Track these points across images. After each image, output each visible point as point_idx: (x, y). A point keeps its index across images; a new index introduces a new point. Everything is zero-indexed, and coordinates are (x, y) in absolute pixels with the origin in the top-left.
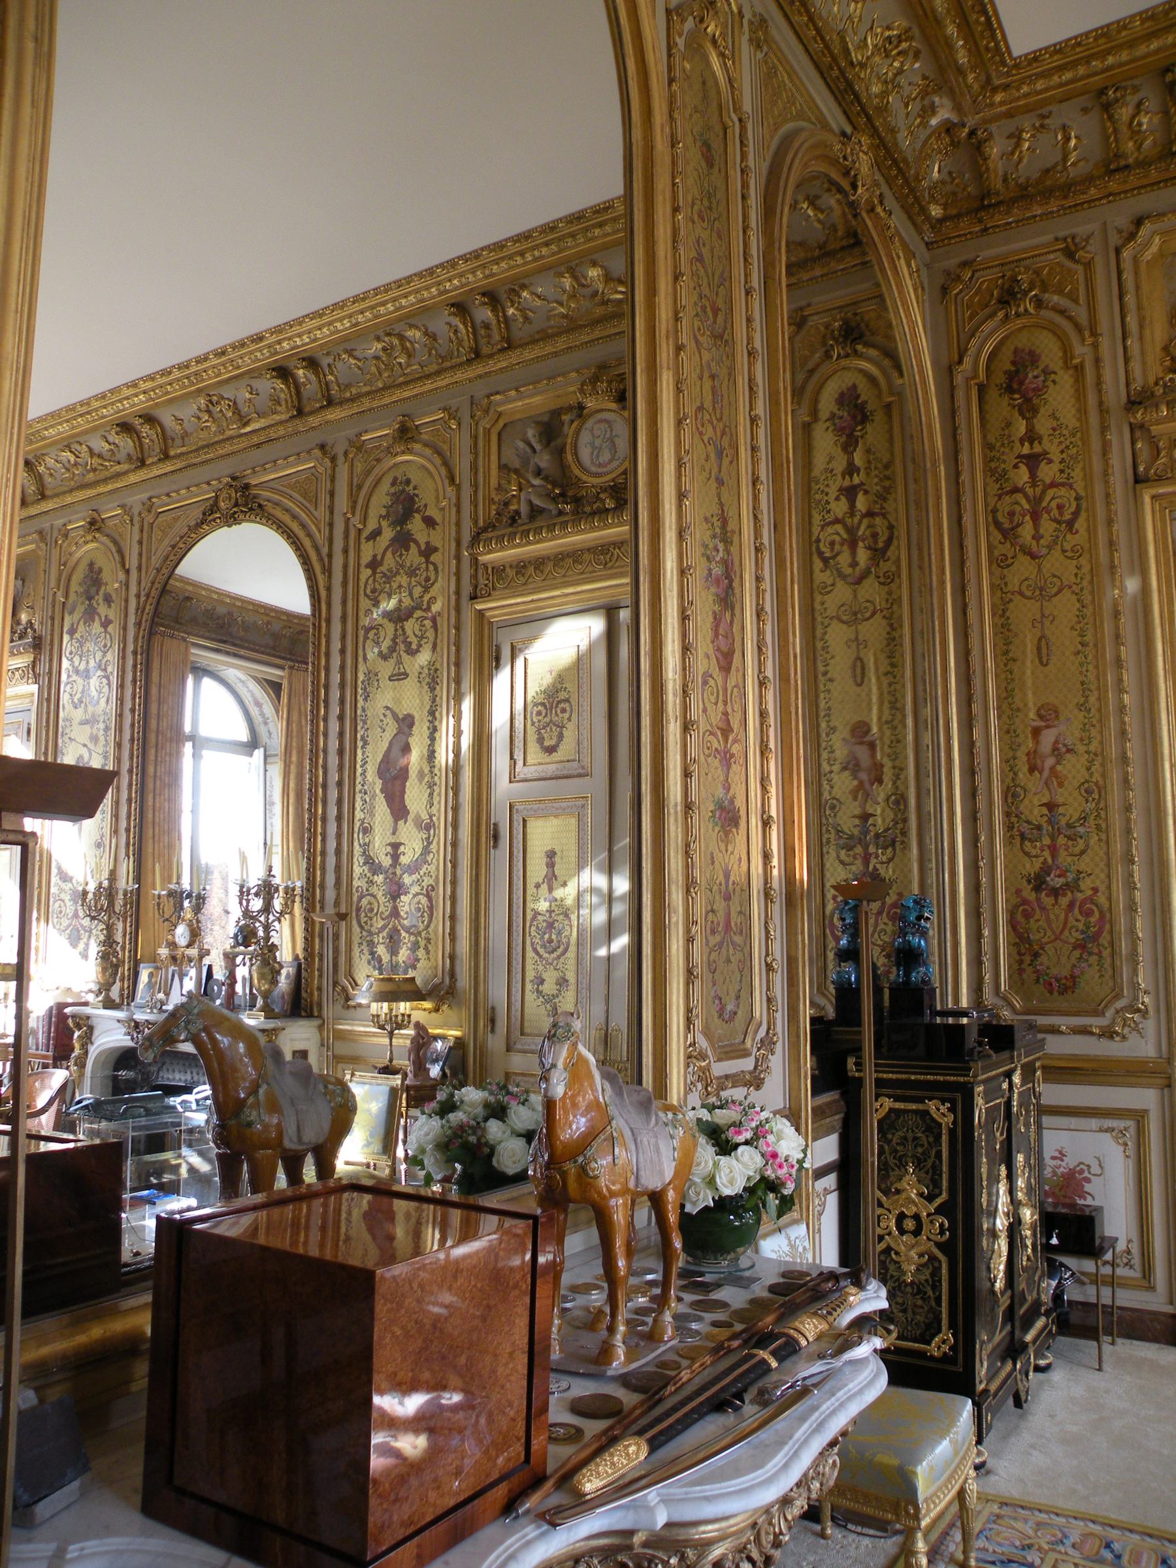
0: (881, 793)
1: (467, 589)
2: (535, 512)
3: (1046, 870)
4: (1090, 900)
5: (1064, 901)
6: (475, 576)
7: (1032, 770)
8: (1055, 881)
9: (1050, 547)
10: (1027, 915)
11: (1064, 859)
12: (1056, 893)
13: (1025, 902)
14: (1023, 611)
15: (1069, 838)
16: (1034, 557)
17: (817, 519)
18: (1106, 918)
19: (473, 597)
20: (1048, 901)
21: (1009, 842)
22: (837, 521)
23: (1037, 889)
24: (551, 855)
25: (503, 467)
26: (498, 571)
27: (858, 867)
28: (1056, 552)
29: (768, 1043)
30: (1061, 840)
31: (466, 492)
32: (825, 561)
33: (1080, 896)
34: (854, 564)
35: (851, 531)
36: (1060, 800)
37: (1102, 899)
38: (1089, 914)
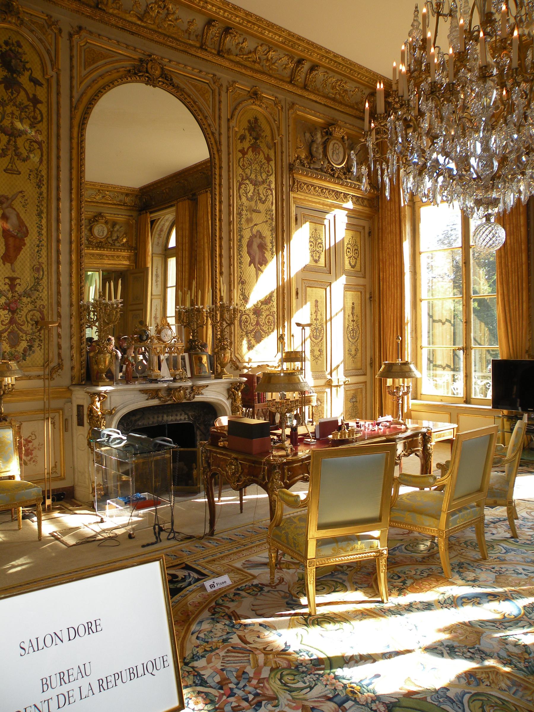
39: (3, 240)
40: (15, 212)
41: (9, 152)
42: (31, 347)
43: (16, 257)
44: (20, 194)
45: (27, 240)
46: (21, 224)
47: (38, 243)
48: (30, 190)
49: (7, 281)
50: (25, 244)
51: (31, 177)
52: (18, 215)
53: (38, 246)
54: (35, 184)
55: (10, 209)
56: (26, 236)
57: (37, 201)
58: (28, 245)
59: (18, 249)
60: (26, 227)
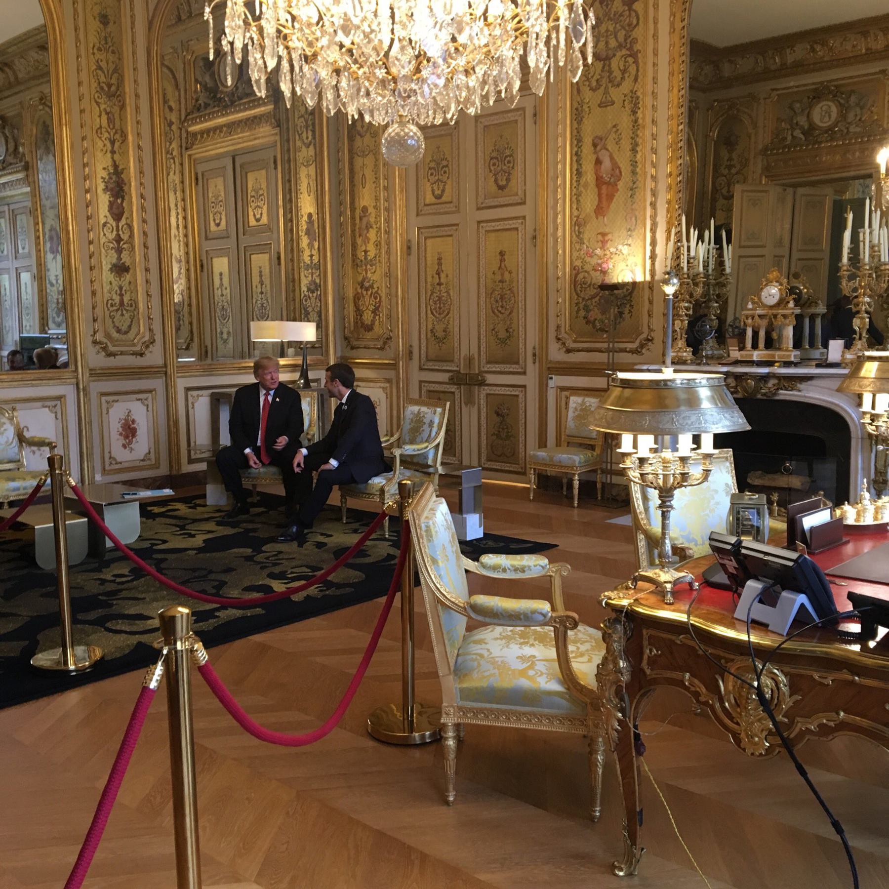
0: (316, 245)
1: (184, 145)
2: (207, 105)
3: (364, 280)
4: (377, 292)
5: (369, 293)
6: (187, 138)
7: (360, 236)
8: (367, 284)
9: (366, 132)
10: (359, 299)
11: (369, 275)
12: (367, 289)
13: (358, 293)
14: (358, 162)
15: (371, 266)
16: (361, 136)
17: (296, 116)
18: (380, 301)
19: (187, 149)
20: (365, 293)
21: (353, 268)
22: (302, 116)
23: (361, 288)
24: (221, 274)
25: (197, 81)
26: (194, 135)
27: (310, 278)
28: (368, 134)
29: (153, 342)
30: (369, 267)
31: (182, 93)
32: (299, 135)
33: (374, 291)
34: (307, 138)
35: (306, 121)
36: (368, 249)
37: (380, 292)
38: (376, 298)
39: (596, 190)
40: (608, 153)
41: (604, 81)
42: (621, 314)
43: (609, 206)
44: (614, 129)
45: (620, 184)
46: (615, 166)
47: (631, 185)
48: (625, 121)
49: (600, 237)
50: (618, 190)
51: (626, 103)
52: (612, 158)
53: (632, 189)
54: (629, 112)
55: (604, 151)
56: (619, 180)
57: (631, 132)
58: (621, 190)
59: (610, 197)
60: (619, 168)
